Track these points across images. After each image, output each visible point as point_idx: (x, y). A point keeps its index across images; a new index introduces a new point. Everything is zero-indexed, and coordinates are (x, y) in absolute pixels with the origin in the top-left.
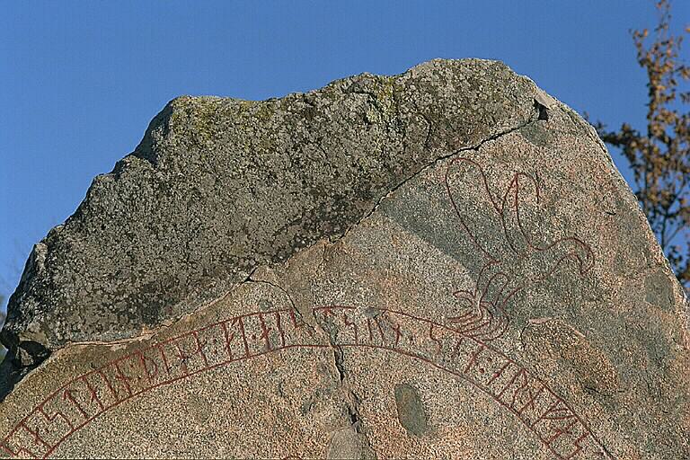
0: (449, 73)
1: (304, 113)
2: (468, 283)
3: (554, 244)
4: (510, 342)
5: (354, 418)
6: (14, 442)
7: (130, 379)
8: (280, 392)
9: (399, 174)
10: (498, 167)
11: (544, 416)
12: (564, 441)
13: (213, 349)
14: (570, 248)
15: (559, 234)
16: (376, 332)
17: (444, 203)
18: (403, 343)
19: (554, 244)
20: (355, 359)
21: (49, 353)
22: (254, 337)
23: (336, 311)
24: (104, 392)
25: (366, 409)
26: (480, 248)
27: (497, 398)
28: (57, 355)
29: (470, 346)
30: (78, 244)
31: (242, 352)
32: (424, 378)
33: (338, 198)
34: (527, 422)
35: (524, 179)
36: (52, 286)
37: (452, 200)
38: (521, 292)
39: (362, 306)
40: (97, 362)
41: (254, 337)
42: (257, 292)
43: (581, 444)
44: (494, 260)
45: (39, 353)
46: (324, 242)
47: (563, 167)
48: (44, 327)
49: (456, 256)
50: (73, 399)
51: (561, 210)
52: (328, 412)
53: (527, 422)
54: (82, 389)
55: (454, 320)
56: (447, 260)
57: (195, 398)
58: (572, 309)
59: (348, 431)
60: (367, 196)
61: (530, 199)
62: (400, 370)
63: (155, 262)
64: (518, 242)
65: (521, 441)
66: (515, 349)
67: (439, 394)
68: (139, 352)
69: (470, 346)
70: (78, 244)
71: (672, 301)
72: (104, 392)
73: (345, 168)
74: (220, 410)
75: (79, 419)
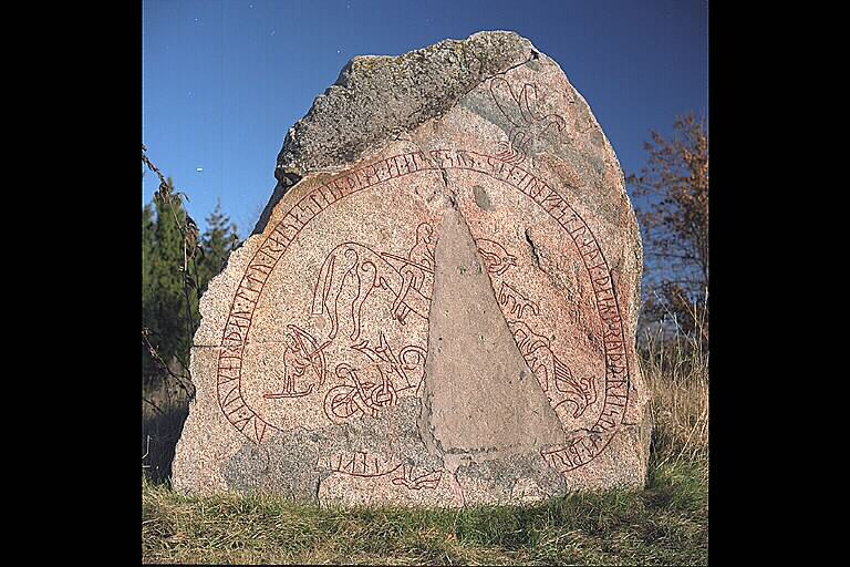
0: (489, 38)
1: (418, 59)
4: (527, 164)
5: (453, 204)
6: (285, 222)
9: (468, 87)
10: (516, 82)
16: (462, 161)
17: (491, 99)
20: (452, 177)
21: (301, 178)
25: (459, 199)
28: (304, 179)
30: (311, 127)
31: (397, 173)
32: (486, 182)
33: (438, 98)
36: (299, 146)
39: (454, 149)
40: (325, 181)
42: (402, 145)
45: (295, 178)
46: (433, 120)
47: (547, 81)
48: (297, 166)
52: (441, 201)
53: (538, 202)
58: (556, 148)
59: (451, 210)
60: (453, 97)
61: (533, 96)
62: (474, 178)
63: (350, 132)
65: (536, 210)
67: (494, 192)
68: (345, 175)
70: (311, 127)
73: (440, 85)
75: (317, 210)
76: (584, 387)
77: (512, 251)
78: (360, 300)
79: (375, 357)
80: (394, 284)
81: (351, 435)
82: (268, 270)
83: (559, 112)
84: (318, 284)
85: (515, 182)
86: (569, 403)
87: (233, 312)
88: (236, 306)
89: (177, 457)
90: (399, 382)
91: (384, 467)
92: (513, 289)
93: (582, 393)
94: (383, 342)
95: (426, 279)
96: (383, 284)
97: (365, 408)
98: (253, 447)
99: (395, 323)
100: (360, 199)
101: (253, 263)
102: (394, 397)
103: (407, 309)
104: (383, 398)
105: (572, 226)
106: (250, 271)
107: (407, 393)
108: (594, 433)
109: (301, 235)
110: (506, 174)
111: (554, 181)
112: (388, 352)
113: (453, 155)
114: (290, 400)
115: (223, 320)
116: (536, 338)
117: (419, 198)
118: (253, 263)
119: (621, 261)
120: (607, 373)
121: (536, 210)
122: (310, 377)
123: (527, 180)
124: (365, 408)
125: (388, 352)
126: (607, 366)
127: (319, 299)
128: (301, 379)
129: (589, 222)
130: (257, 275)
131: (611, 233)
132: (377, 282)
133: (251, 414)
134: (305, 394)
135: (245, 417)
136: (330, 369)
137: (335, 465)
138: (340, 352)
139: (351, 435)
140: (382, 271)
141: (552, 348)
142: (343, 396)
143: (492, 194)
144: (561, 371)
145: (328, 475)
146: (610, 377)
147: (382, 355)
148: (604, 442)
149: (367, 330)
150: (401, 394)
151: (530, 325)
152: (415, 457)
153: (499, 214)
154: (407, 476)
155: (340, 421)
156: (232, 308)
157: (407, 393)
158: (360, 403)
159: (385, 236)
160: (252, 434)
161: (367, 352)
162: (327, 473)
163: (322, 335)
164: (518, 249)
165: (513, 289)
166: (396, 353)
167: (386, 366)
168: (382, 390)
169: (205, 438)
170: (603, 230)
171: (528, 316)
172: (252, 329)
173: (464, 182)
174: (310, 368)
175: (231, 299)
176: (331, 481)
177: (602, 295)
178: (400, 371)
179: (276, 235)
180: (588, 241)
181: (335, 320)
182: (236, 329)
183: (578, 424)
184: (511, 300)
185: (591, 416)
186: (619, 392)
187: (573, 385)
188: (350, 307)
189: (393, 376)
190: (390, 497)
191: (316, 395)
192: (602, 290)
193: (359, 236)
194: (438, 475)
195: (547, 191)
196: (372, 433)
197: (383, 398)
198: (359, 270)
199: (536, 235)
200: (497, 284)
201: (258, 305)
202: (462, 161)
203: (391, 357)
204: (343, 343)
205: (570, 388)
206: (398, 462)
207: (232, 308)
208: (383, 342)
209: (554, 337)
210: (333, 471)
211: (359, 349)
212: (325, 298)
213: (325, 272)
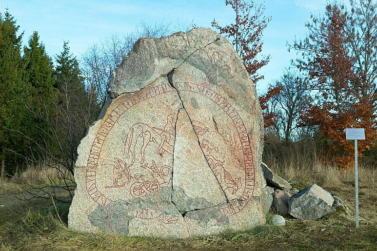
2: (205, 76)
4: (214, 88)
6: (112, 114)
10: (210, 51)
12: (226, 108)
15: (223, 65)
16: (186, 88)
17: (199, 59)
20: (182, 93)
24: (130, 103)
26: (207, 68)
29: (206, 89)
31: (158, 93)
32: (197, 96)
34: (218, 104)
37: (201, 58)
38: (215, 77)
49: (202, 71)
51: (224, 59)
53: (218, 104)
54: (126, 103)
55: (202, 84)
64: (215, 66)
67: (200, 100)
69: (206, 89)
71: (247, 77)
72: (130, 103)
76: (236, 182)
77: (207, 126)
78: (144, 146)
79: (150, 170)
80: (159, 141)
81: (141, 202)
82: (105, 135)
84: (126, 139)
89: (70, 213)
90: (161, 181)
93: (235, 184)
96: (153, 140)
97: (147, 191)
98: (101, 208)
100: (144, 104)
101: (99, 132)
102: (159, 187)
103: (164, 151)
104: (154, 187)
105: (232, 115)
106: (98, 135)
107: (164, 185)
108: (240, 201)
109: (119, 120)
110: (205, 92)
111: (226, 95)
112: (156, 169)
113: (183, 85)
115: (88, 156)
116: (217, 162)
118: (99, 132)
119: (252, 130)
121: (217, 107)
123: (214, 95)
124: (147, 191)
125: (156, 169)
127: (127, 147)
128: (120, 180)
132: (151, 140)
133: (100, 194)
134: (122, 186)
135: (98, 196)
136: (133, 176)
137: (135, 215)
138: (136, 170)
139: (141, 202)
140: (153, 135)
143: (199, 101)
144: (227, 175)
145: (132, 219)
146: (247, 177)
147: (154, 169)
148: (244, 204)
152: (168, 211)
153: (202, 110)
154: (164, 219)
155: (136, 197)
156: (91, 151)
157: (164, 185)
158: (145, 190)
159: (154, 120)
160: (101, 203)
162: (131, 218)
164: (210, 125)
166: (159, 169)
167: (156, 175)
170: (245, 116)
173: (187, 95)
175: (90, 147)
177: (244, 144)
179: (109, 120)
183: (234, 197)
185: (239, 193)
186: (251, 183)
188: (140, 150)
189: (158, 178)
191: (127, 186)
192: (244, 142)
195: (222, 100)
196: (151, 203)
197: (154, 187)
200: (201, 140)
202: (186, 88)
203: (157, 171)
204: (137, 165)
207: (91, 151)
209: (224, 161)
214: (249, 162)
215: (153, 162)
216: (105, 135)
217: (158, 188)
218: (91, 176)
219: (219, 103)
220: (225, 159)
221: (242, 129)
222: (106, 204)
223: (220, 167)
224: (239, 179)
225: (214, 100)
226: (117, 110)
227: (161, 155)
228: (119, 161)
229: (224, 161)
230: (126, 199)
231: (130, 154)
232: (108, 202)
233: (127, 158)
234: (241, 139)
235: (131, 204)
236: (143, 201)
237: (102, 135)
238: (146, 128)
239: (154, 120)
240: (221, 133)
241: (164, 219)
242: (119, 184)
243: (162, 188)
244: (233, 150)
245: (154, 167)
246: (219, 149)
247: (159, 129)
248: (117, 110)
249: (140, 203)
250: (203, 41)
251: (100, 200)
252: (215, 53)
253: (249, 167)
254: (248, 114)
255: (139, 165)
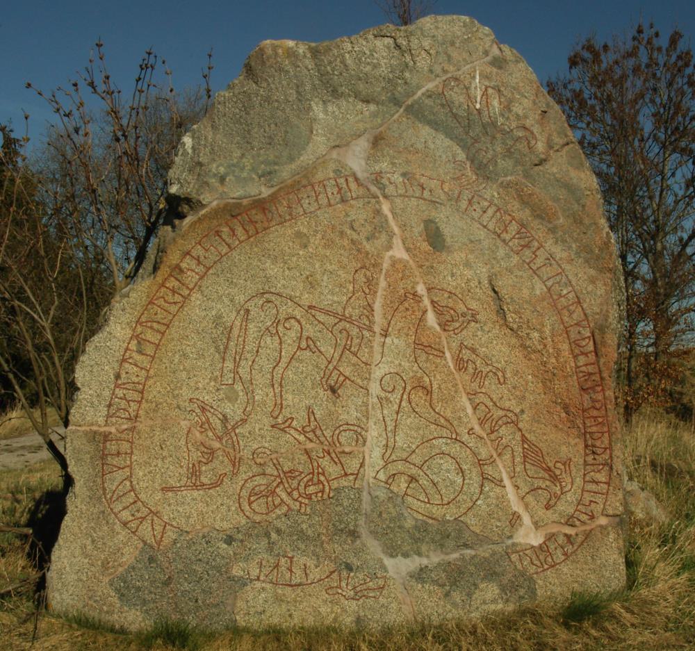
2: (461, 156)
3: (512, 130)
6: (183, 265)
7: (256, 222)
8: (352, 228)
11: (514, 238)
12: (527, 252)
13: (307, 201)
14: (520, 134)
15: (514, 125)
17: (443, 105)
18: (426, 194)
19: (512, 130)
22: (333, 193)
23: (383, 175)
24: (240, 231)
27: (485, 227)
29: (466, 195)
34: (504, 241)
35: (490, 91)
37: (448, 105)
38: (493, 161)
41: (333, 193)
43: (537, 253)
44: (476, 141)
50: (220, 237)
51: (514, 109)
53: (504, 241)
54: (225, 230)
56: (448, 142)
57: (299, 235)
61: (496, 103)
64: (490, 128)
66: (493, 196)
67: (452, 225)
72: (240, 231)
74: (316, 241)
75: (225, 250)
76: (558, 472)
77: (474, 305)
78: (283, 365)
79: (302, 438)
80: (328, 350)
81: (274, 536)
82: (162, 328)
83: (528, 123)
85: (476, 215)
86: (540, 491)
87: (120, 382)
88: (123, 375)
90: (333, 470)
91: (315, 574)
92: (473, 350)
93: (555, 479)
94: (312, 419)
95: (365, 340)
96: (308, 344)
97: (289, 501)
99: (323, 394)
100: (280, 237)
103: (342, 378)
104: (311, 489)
105: (546, 272)
106: (139, 329)
107: (344, 482)
109: (204, 283)
110: (464, 204)
111: (525, 214)
113: (397, 178)
114: (196, 494)
115: (107, 393)
116: (501, 413)
117: (355, 236)
120: (586, 455)
121: (501, 252)
122: (221, 465)
123: (490, 212)
124: (289, 501)
125: (318, 432)
126: (586, 446)
127: (229, 365)
128: (210, 466)
129: (567, 267)
130: (149, 335)
131: (593, 281)
132: (304, 345)
134: (217, 484)
135: (139, 515)
136: (246, 453)
139: (274, 536)
140: (310, 331)
141: (521, 425)
142: (262, 488)
143: (447, 231)
147: (311, 435)
149: (291, 403)
150: (335, 485)
151: (495, 397)
154: (343, 584)
155: (258, 518)
156: (118, 376)
157: (344, 482)
159: (311, 282)
161: (292, 432)
162: (243, 582)
163: (233, 411)
164: (480, 303)
165: (473, 350)
166: (328, 433)
168: (311, 480)
169: (89, 542)
171: (491, 385)
172: (144, 405)
174: (220, 453)
175: (116, 365)
176: (249, 592)
178: (333, 455)
179: (172, 283)
180: (565, 292)
181: (249, 392)
182: (123, 404)
184: (470, 366)
185: (566, 506)
186: (602, 477)
187: (544, 470)
188: (269, 376)
189: (325, 462)
190: (323, 610)
192: (583, 353)
193: (279, 286)
194: (381, 582)
195: (514, 228)
196: (302, 536)
197: (311, 489)
198: (280, 328)
199: (504, 284)
201: (152, 372)
203: (322, 439)
204: (263, 421)
205: (542, 474)
206: (332, 567)
208: (312, 419)
209: (522, 411)
210: (251, 581)
211: (280, 427)
212: (237, 365)
213: (236, 332)
214: (595, 413)
215: (310, 411)
216: (162, 328)
217: (323, 491)
218: (118, 454)
219: (507, 237)
220: (525, 405)
221: (575, 316)
222: (166, 541)
223: (511, 428)
224: (564, 464)
225: (491, 226)
226: (198, 251)
227: (333, 390)
228: (203, 410)
229: (522, 411)
230: (226, 525)
231: (238, 387)
232: (171, 535)
233: (229, 399)
234: (575, 344)
235: (242, 541)
236: (279, 531)
237: (151, 328)
238: (287, 309)
239: (311, 282)
240: (515, 326)
241: (343, 584)
242: (204, 480)
243: (338, 490)
244: (547, 378)
245: (312, 429)
246: (508, 375)
247: (327, 313)
248: (198, 251)
249: (268, 535)
250: (454, 54)
251: (145, 530)
252: (490, 91)
253: (594, 429)
254: (592, 272)
255: (267, 421)
